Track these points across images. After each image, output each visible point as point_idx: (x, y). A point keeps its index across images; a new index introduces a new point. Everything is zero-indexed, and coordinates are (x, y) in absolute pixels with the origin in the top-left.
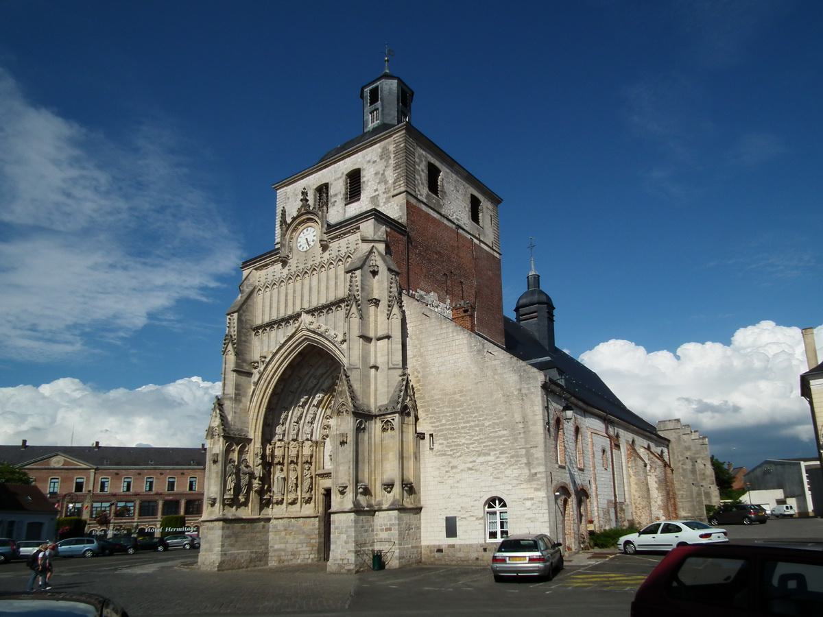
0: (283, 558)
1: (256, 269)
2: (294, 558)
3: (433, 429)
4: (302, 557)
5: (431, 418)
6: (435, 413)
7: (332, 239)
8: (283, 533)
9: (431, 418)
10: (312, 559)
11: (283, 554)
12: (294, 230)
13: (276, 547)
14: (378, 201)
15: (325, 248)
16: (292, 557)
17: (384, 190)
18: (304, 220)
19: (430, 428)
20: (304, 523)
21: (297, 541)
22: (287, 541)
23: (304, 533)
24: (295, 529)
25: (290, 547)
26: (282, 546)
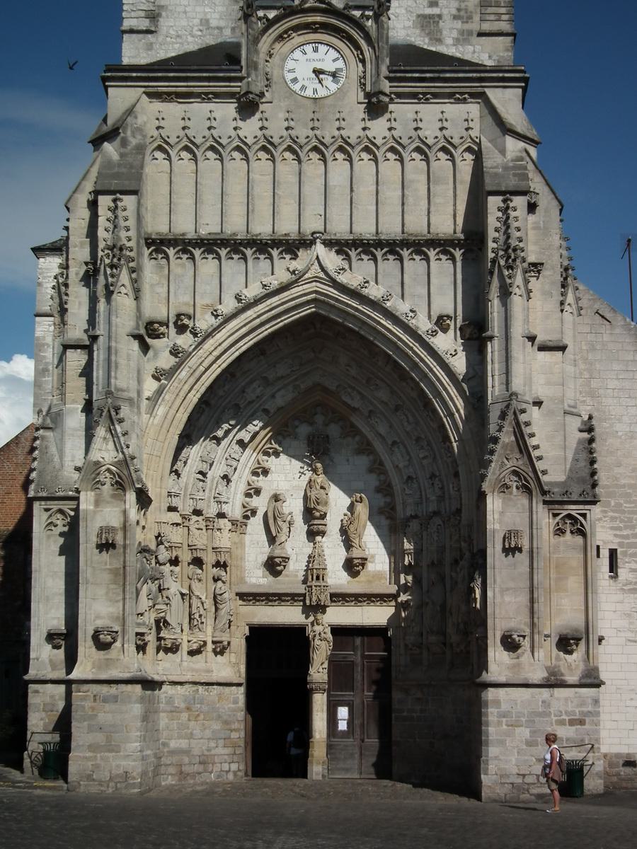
0: (186, 769)
1: (150, 95)
2: (205, 771)
3: (618, 540)
4: (217, 768)
5: (613, 519)
6: (624, 512)
7: (399, 95)
8: (185, 716)
9: (613, 519)
10: (235, 773)
11: (186, 760)
12: (280, 38)
13: (173, 744)
14: (440, 31)
15: (375, 107)
16: (201, 768)
17: (454, 12)
18: (315, 23)
19: (611, 538)
20: (220, 696)
21: (208, 733)
22: (191, 734)
23: (219, 717)
24: (205, 708)
25: (198, 747)
26: (183, 744)
